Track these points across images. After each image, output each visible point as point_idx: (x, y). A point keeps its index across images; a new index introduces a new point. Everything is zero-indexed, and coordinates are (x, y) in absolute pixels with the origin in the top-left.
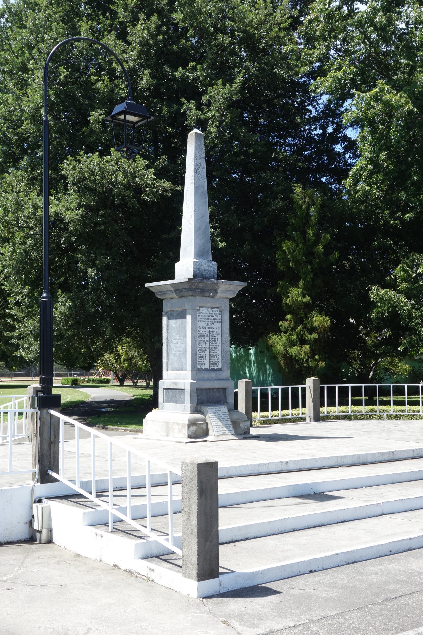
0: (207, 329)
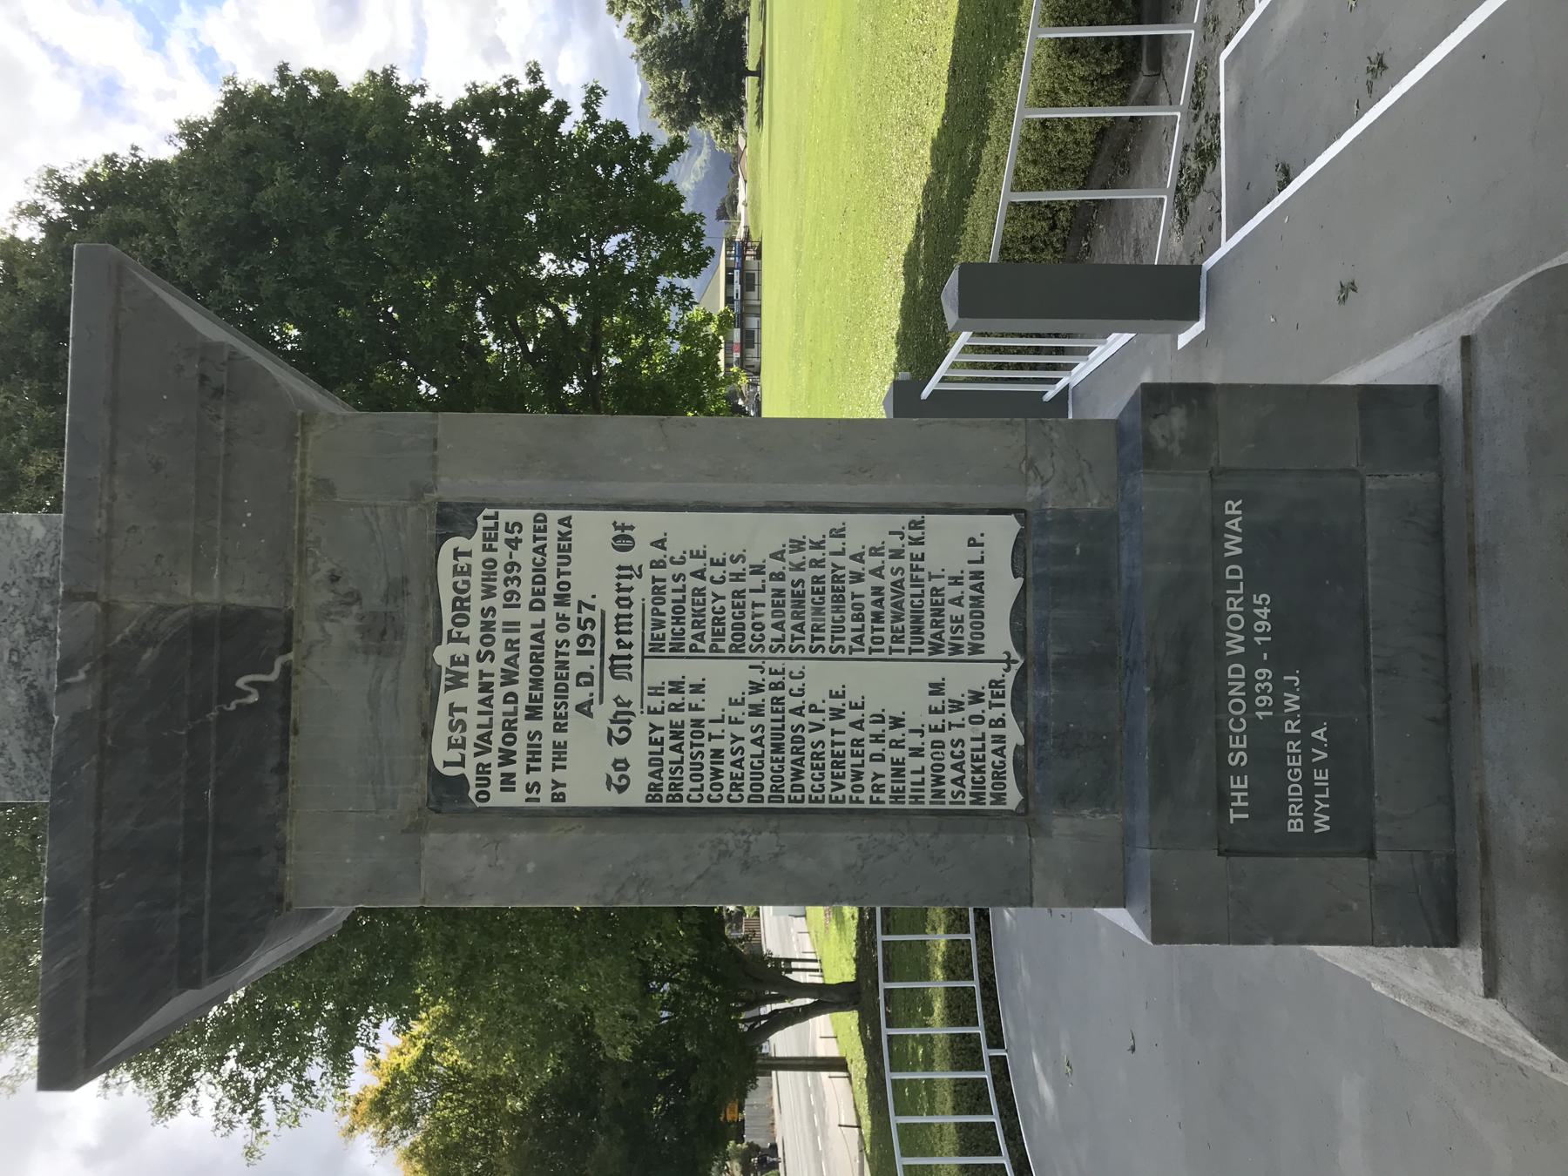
0: (629, 690)
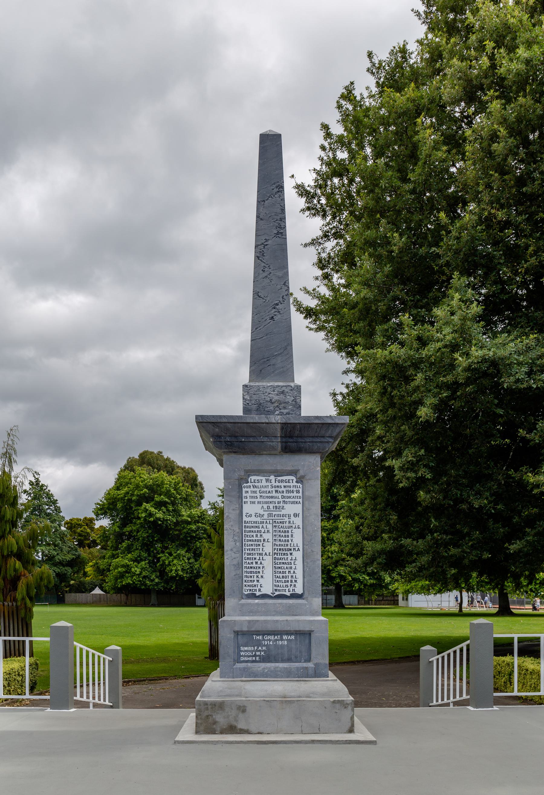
0: (266, 517)
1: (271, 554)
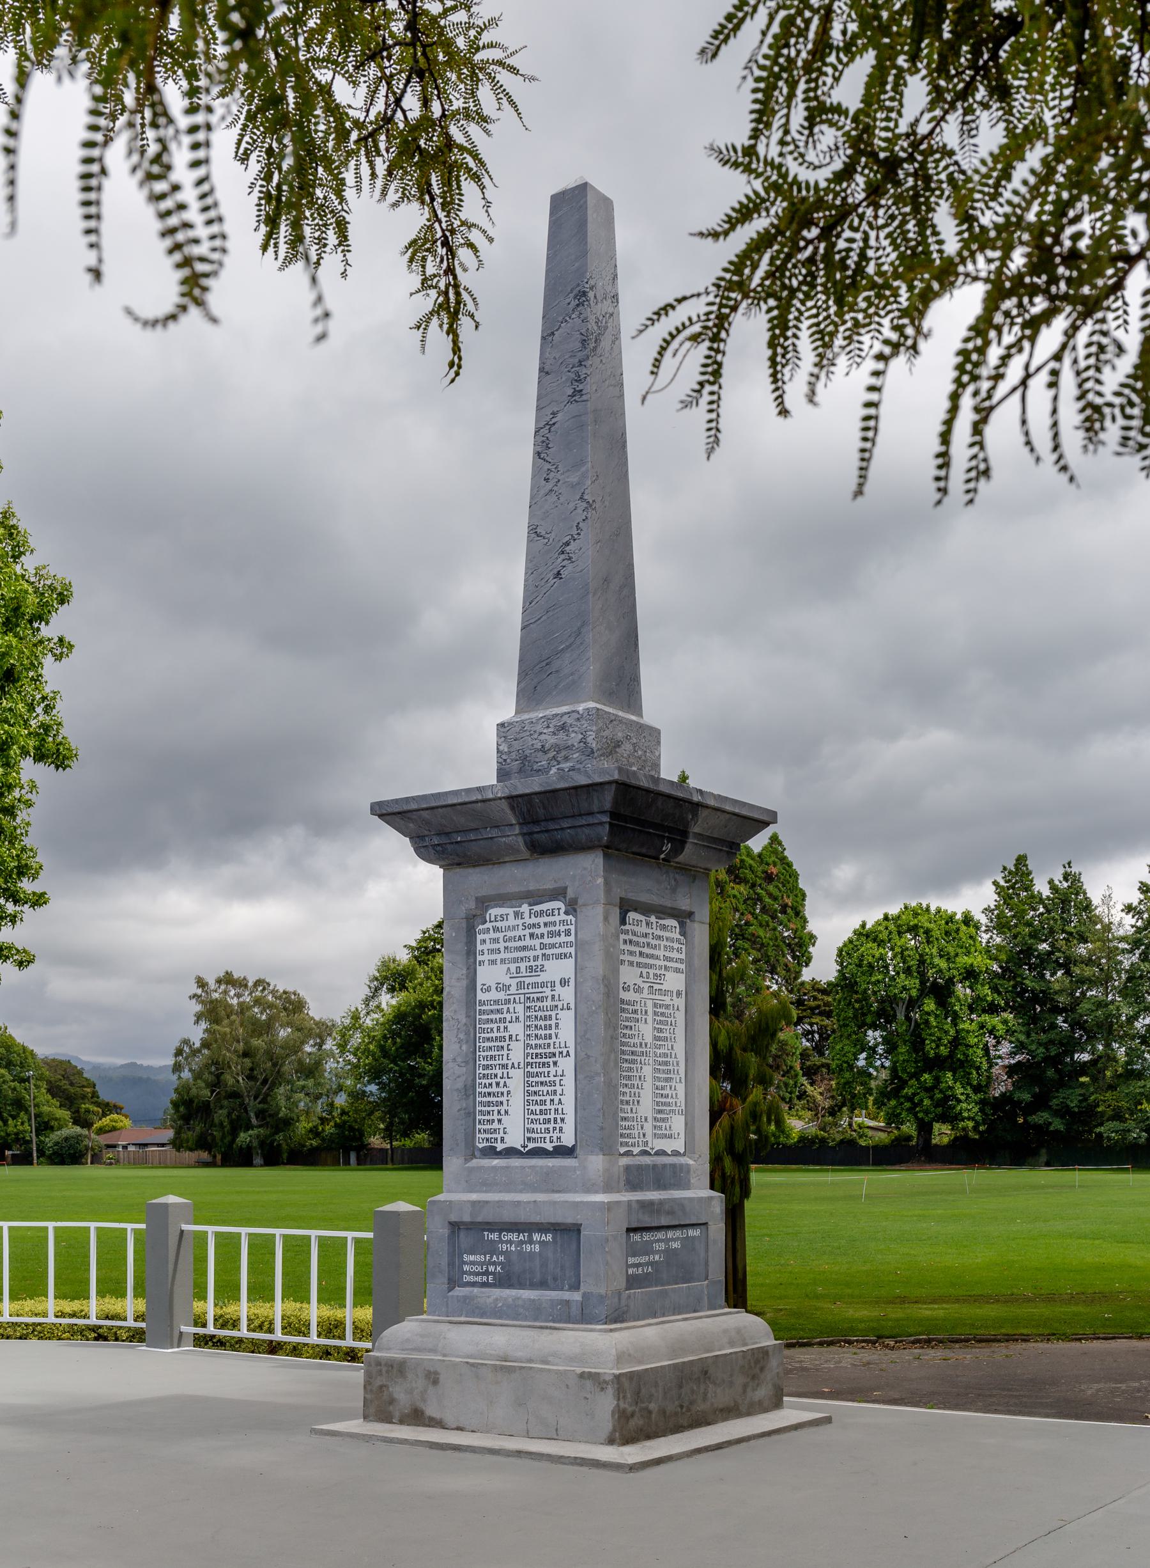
0: (513, 990)
1: (522, 1065)
